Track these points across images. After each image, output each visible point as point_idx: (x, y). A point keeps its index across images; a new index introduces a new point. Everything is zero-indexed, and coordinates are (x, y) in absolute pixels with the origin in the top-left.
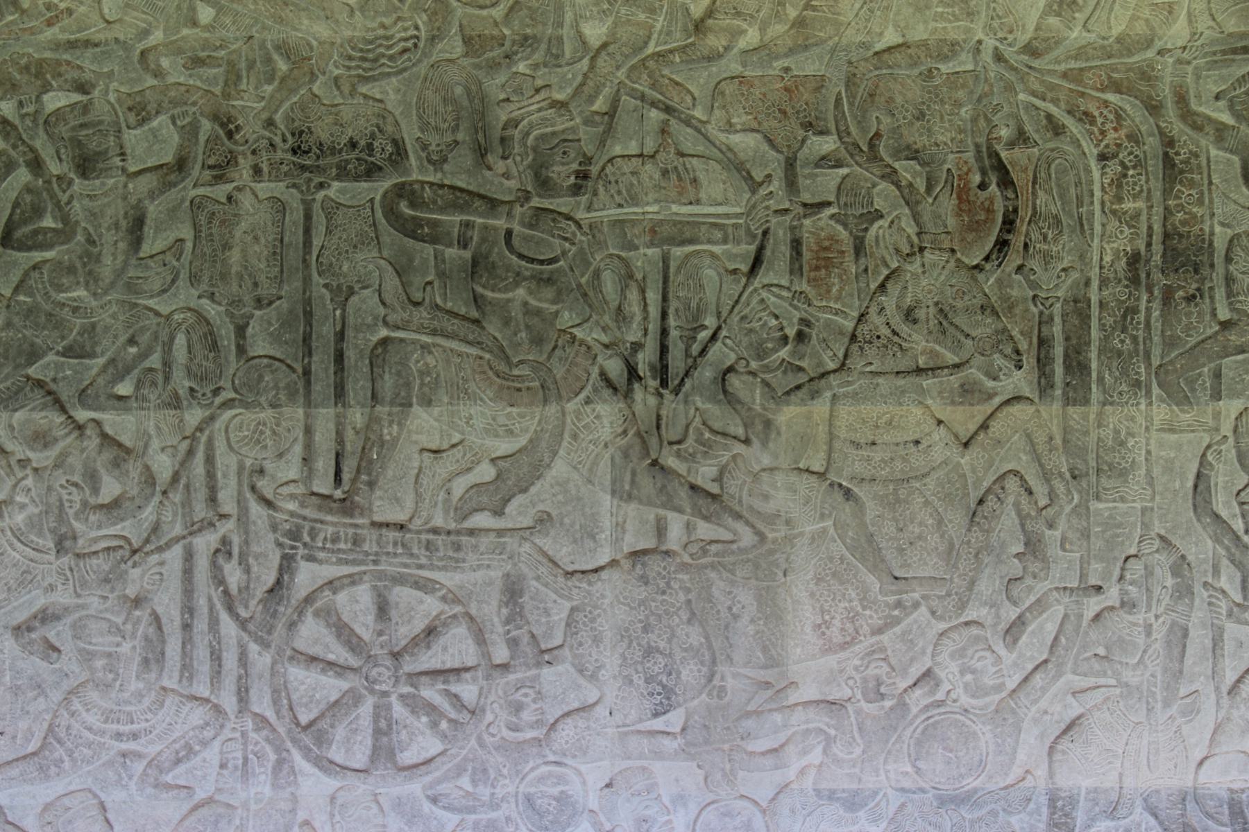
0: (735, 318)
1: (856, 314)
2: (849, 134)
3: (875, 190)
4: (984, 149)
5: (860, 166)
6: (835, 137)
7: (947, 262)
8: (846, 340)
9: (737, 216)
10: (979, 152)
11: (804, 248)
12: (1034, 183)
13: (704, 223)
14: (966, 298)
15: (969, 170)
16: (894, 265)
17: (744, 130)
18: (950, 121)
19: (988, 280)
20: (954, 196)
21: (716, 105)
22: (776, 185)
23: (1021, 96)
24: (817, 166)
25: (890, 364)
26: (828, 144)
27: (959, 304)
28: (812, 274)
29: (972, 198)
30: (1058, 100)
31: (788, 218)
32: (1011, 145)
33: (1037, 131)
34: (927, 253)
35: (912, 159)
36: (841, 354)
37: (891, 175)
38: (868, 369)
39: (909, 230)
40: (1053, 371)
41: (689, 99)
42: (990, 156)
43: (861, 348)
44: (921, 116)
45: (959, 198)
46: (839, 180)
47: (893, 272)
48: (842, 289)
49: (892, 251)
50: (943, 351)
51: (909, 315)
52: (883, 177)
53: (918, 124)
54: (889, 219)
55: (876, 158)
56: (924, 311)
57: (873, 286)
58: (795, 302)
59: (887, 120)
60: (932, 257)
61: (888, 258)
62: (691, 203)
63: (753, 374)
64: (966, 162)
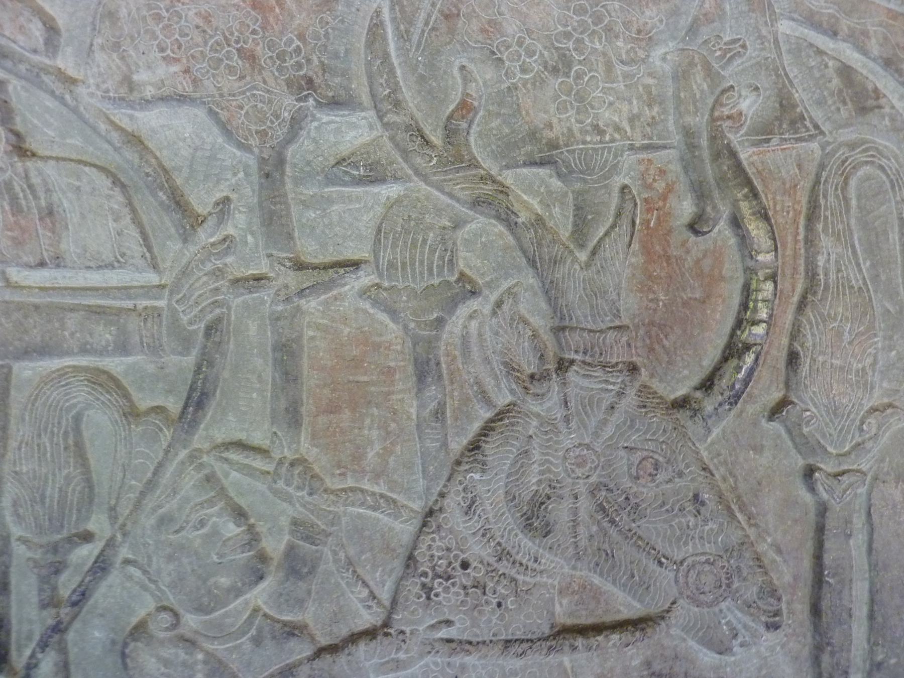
0: (148, 521)
1: (417, 505)
2: (397, 104)
3: (462, 234)
4: (704, 142)
5: (425, 178)
6: (372, 114)
7: (620, 394)
8: (398, 564)
9: (149, 291)
10: (692, 147)
11: (305, 363)
12: (812, 217)
13: (73, 309)
14: (660, 477)
15: (670, 189)
16: (503, 399)
17: (163, 99)
18: (626, 76)
19: (709, 431)
20: (636, 246)
21: (99, 41)
22: (238, 224)
23: (785, 27)
24: (330, 181)
25: (490, 624)
26: (354, 131)
27: (646, 491)
28: (322, 420)
29: (674, 252)
30: (865, 34)
31: (266, 295)
32: (764, 132)
33: (821, 102)
34: (571, 375)
35: (542, 163)
36: (385, 596)
37: (494, 202)
38: (443, 633)
39: (537, 321)
40: (848, 636)
41: (37, 29)
42: (716, 156)
43: (427, 589)
44: (561, 65)
45: (647, 250)
46: (380, 210)
47: (500, 416)
48: (387, 452)
49: (499, 368)
50: (608, 587)
51: (535, 517)
52: (476, 203)
53: (555, 83)
54: (494, 297)
55: (459, 158)
56: (567, 504)
57: (457, 445)
58: (281, 484)
59: (484, 74)
60: (586, 383)
61: (489, 383)
62: (42, 264)
63: (190, 643)
64: (662, 172)
